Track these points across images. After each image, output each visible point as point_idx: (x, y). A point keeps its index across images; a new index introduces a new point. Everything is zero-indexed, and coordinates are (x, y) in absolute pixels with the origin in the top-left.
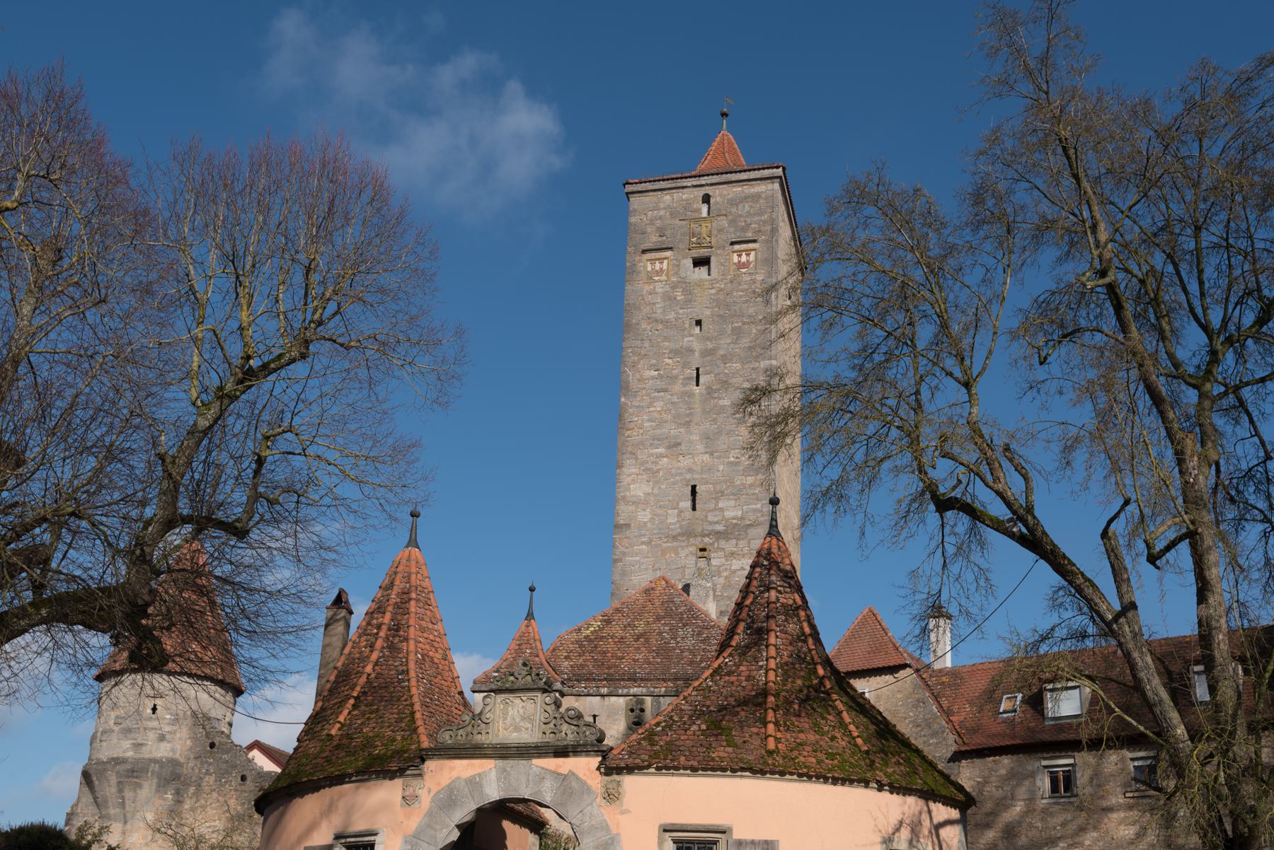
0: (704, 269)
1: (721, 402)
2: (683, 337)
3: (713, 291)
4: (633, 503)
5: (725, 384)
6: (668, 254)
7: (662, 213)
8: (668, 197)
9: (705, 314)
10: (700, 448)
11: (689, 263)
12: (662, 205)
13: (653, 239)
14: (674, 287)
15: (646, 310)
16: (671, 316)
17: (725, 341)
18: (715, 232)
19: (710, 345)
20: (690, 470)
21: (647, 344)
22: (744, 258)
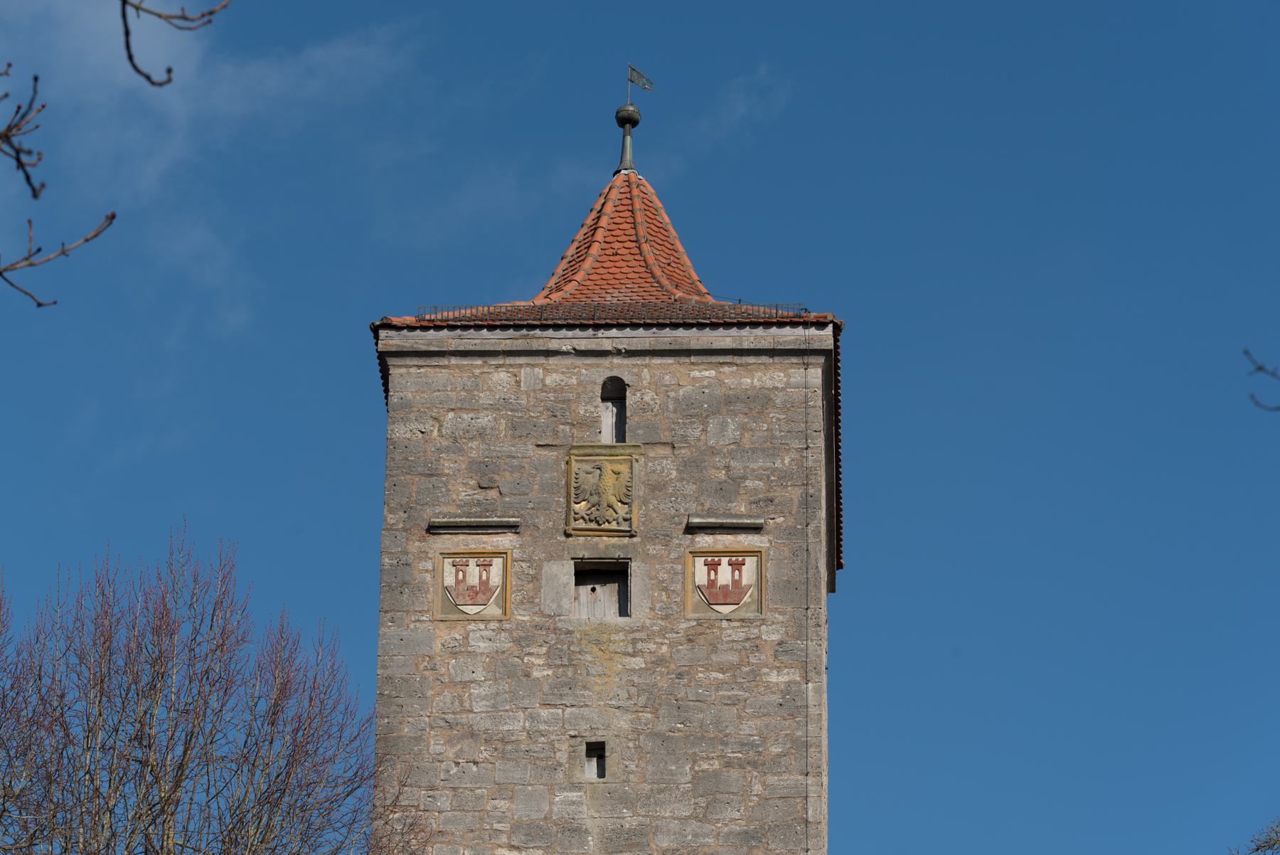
0: (607, 594)
2: (552, 789)
3: (638, 663)
6: (505, 541)
7: (485, 420)
8: (502, 376)
9: (615, 727)
11: (566, 571)
12: (484, 398)
13: (460, 495)
14: (523, 640)
16: (516, 725)
17: (673, 811)
18: (639, 491)
19: (630, 820)
22: (725, 575)
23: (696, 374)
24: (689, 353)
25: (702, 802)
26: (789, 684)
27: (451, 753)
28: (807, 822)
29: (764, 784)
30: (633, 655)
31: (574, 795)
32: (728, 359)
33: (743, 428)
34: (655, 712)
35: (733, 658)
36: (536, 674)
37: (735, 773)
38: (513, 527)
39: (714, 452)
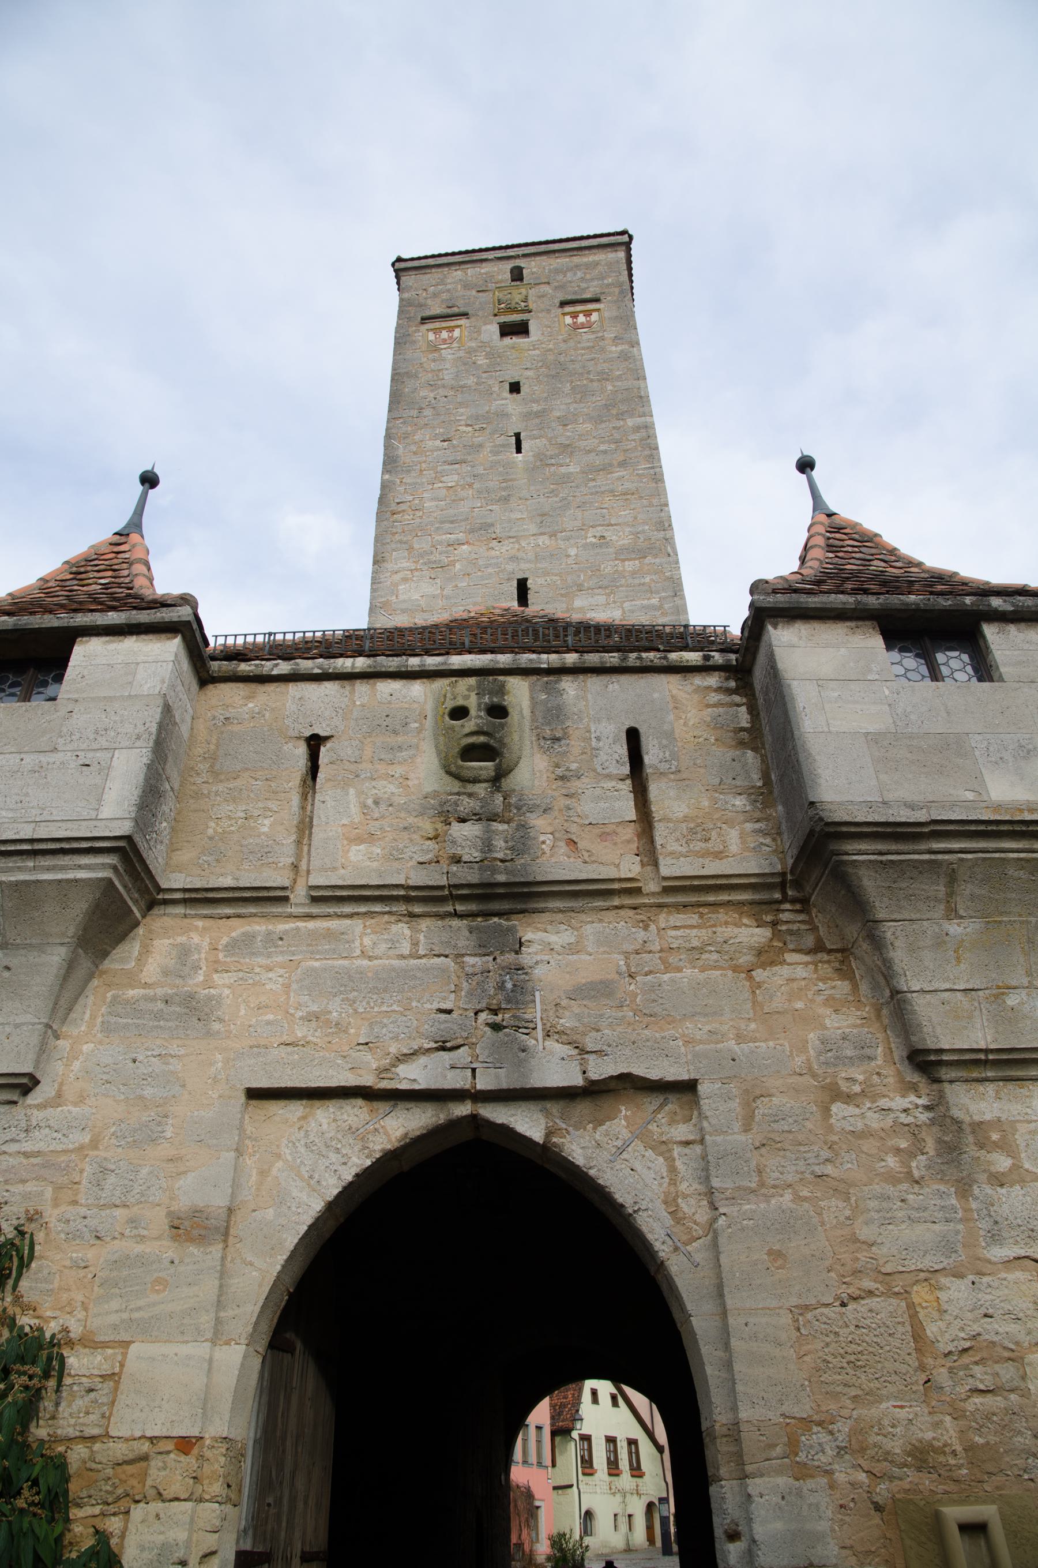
1: (563, 470)
3: (537, 352)
4: (404, 611)
5: (567, 449)
6: (462, 322)
7: (449, 287)
8: (459, 273)
10: (533, 528)
11: (495, 329)
15: (424, 377)
16: (471, 381)
19: (535, 407)
20: (513, 559)
21: (428, 412)
23: (558, 260)
24: (554, 251)
25: (579, 396)
26: (622, 351)
27: (432, 395)
28: (641, 397)
29: (614, 386)
30: (534, 350)
31: (503, 402)
32: (575, 253)
33: (585, 273)
34: (548, 368)
35: (591, 344)
36: (479, 362)
37: (595, 384)
38: (465, 315)
39: (570, 282)
